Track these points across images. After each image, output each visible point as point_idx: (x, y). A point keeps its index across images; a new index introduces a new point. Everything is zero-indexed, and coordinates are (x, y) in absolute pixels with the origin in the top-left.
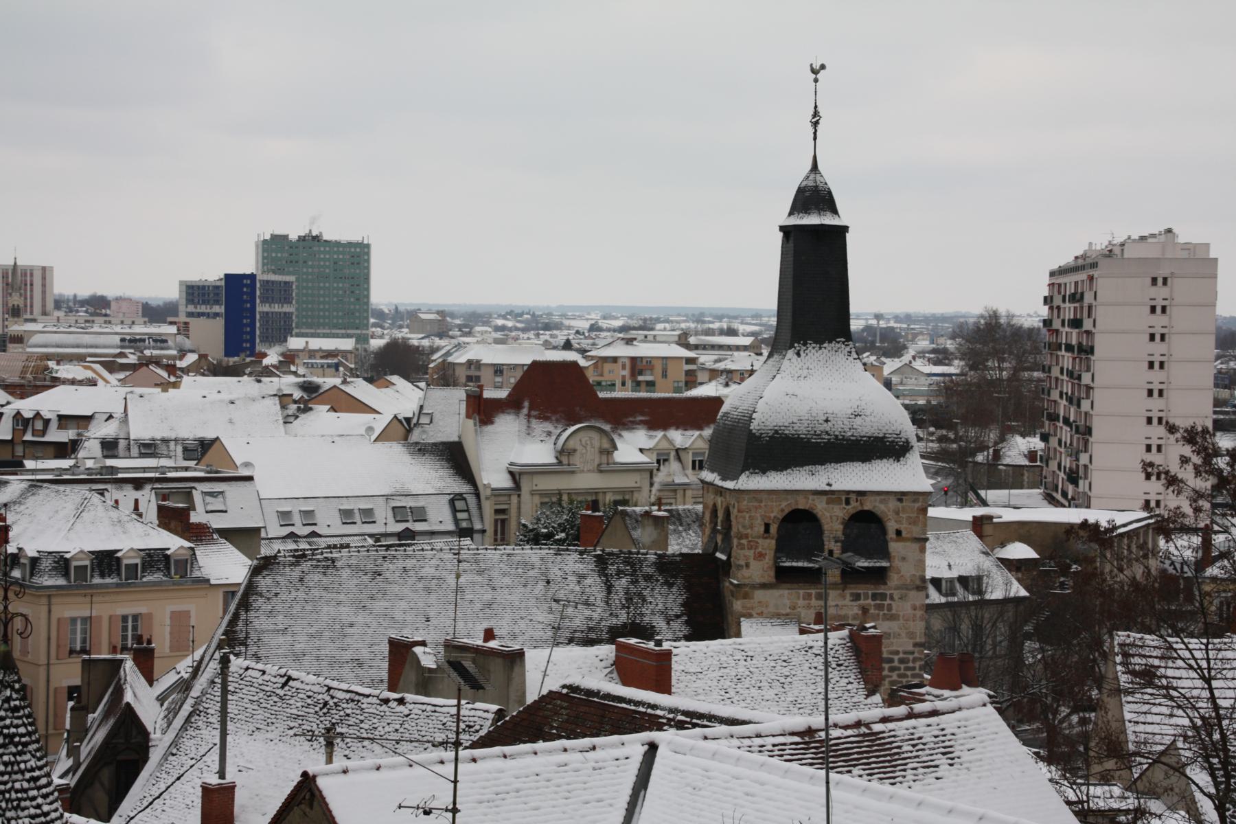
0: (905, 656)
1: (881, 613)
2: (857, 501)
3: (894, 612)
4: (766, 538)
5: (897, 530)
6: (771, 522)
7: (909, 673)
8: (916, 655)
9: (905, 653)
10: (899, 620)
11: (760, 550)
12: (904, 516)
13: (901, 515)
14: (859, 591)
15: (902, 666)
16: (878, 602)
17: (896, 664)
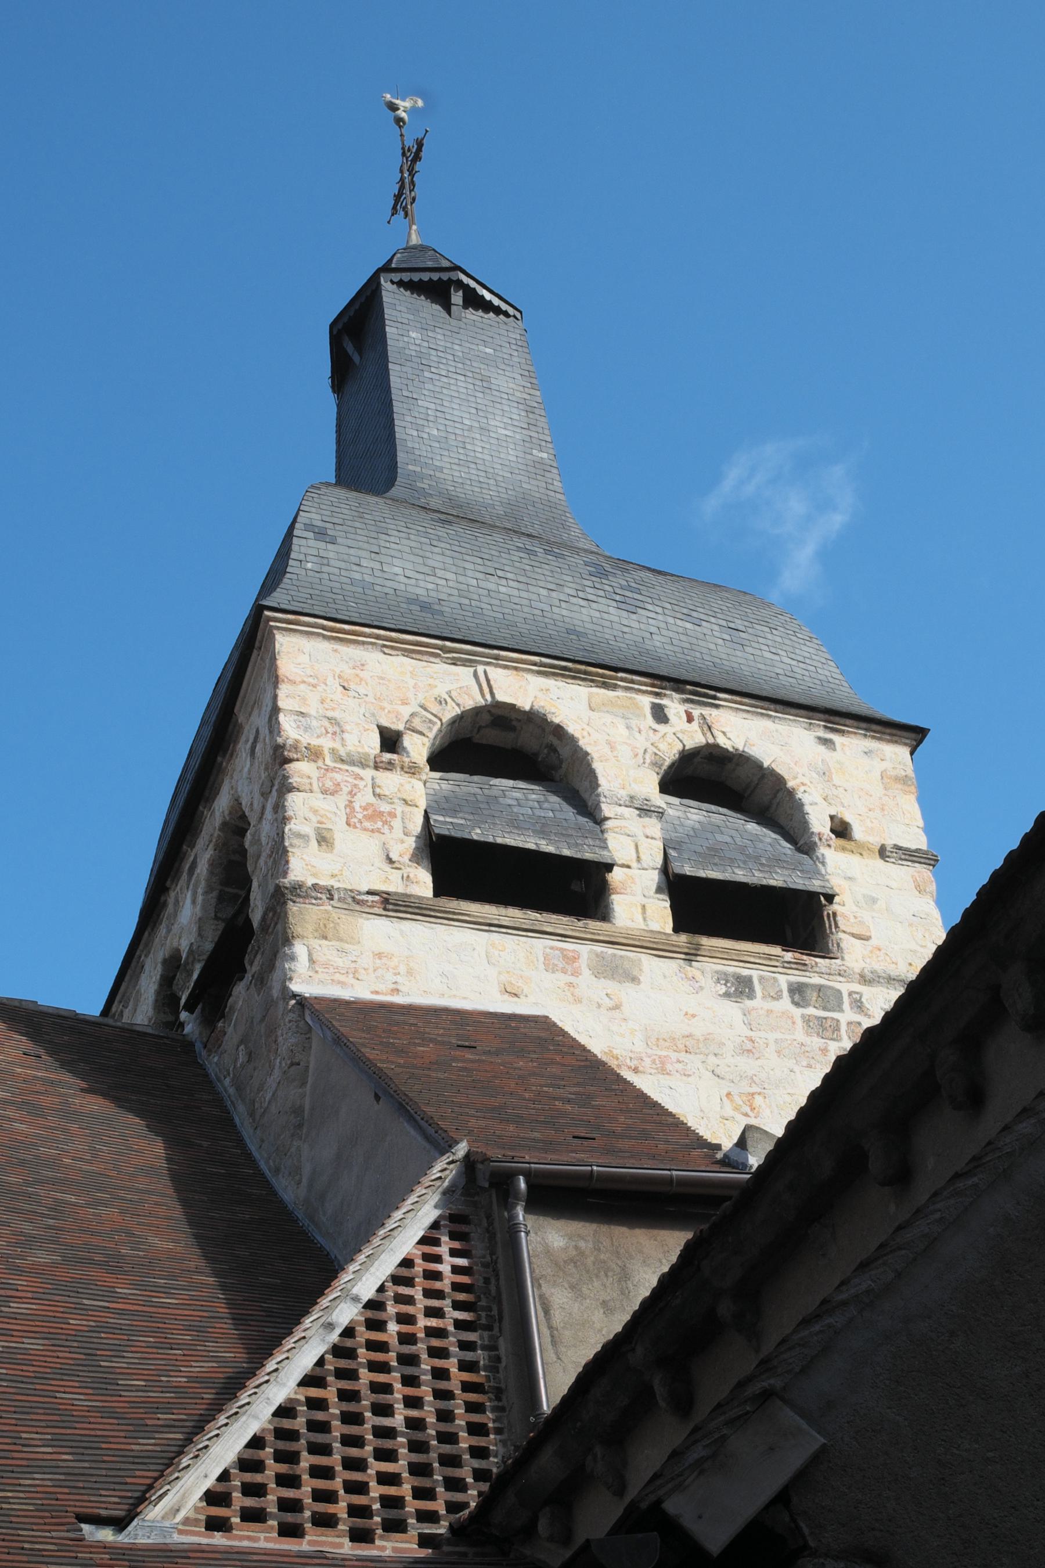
2: (690, 719)
4: (390, 766)
14: (745, 972)
16: (811, 1011)
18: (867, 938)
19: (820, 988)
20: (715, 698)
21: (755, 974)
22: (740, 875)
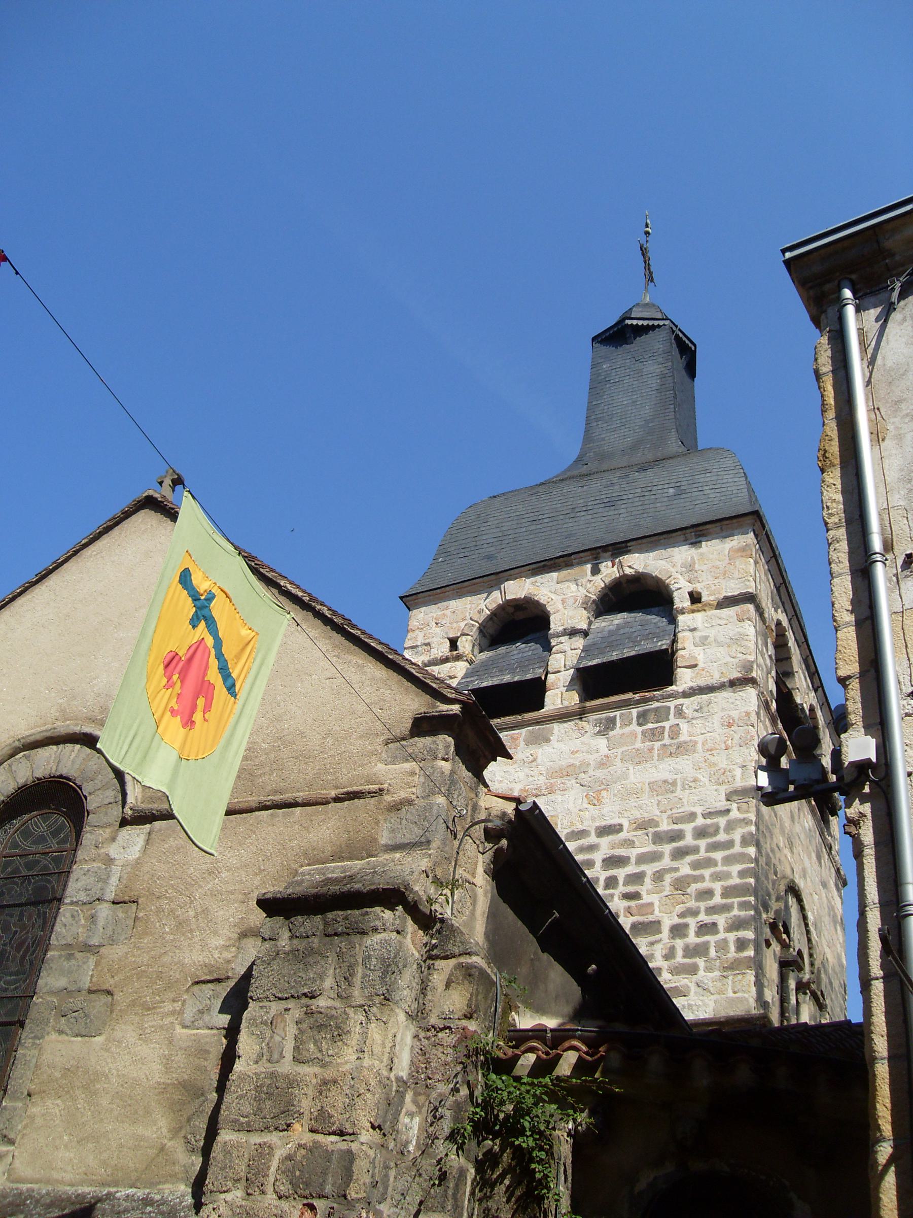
0: (709, 821)
1: (657, 745)
5: (691, 594)
7: (718, 855)
8: (735, 814)
12: (704, 568)
13: (697, 567)
14: (612, 715)
15: (703, 843)
16: (650, 726)
17: (689, 840)
18: (696, 666)
19: (657, 709)
20: (627, 547)
22: (615, 656)
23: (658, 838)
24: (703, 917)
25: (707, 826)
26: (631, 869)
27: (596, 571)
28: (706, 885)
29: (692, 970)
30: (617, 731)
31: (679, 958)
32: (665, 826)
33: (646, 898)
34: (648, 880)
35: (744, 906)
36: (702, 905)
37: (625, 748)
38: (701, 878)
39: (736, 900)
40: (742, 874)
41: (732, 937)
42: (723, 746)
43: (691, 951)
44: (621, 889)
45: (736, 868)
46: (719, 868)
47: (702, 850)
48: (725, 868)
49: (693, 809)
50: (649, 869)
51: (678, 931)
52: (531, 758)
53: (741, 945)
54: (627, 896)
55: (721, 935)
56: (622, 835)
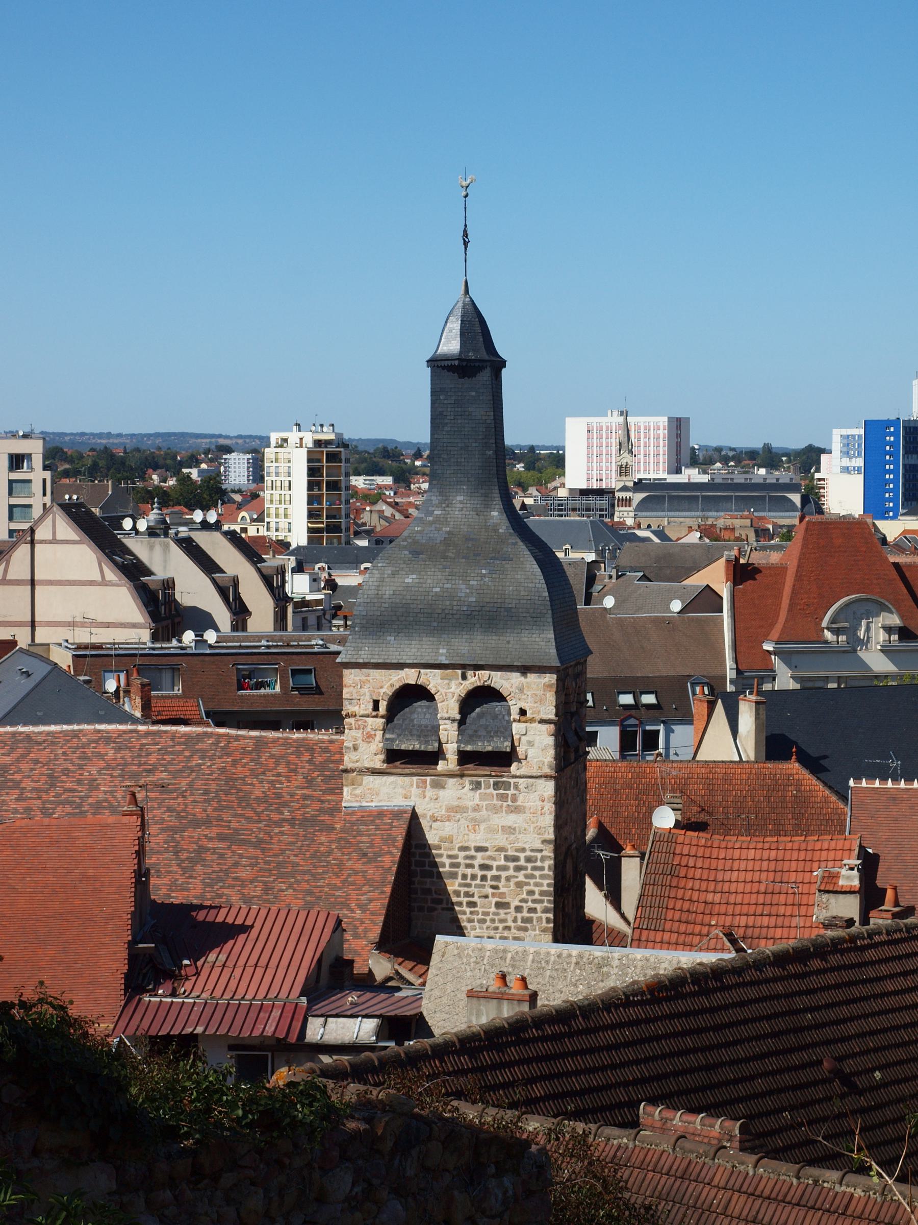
0: (533, 854)
1: (505, 804)
3: (519, 803)
5: (521, 709)
6: (380, 698)
7: (537, 873)
9: (532, 850)
10: (525, 813)
11: (369, 729)
13: (525, 692)
14: (479, 780)
15: (529, 865)
16: (501, 791)
17: (522, 862)
19: (504, 782)
21: (482, 780)
23: (507, 858)
24: (530, 904)
25: (532, 857)
26: (494, 872)
27: (464, 677)
28: (532, 888)
29: (525, 929)
30: (482, 791)
31: (519, 923)
32: (510, 853)
33: (502, 890)
34: (503, 880)
35: (549, 901)
36: (530, 898)
37: (487, 802)
38: (528, 884)
39: (546, 898)
40: (548, 885)
41: (544, 916)
42: (539, 812)
43: (525, 920)
44: (489, 883)
45: (546, 882)
46: (538, 880)
47: (529, 869)
48: (540, 881)
49: (524, 846)
50: (504, 874)
51: (518, 909)
52: (435, 797)
53: (548, 920)
54: (493, 887)
55: (539, 914)
56: (488, 853)
